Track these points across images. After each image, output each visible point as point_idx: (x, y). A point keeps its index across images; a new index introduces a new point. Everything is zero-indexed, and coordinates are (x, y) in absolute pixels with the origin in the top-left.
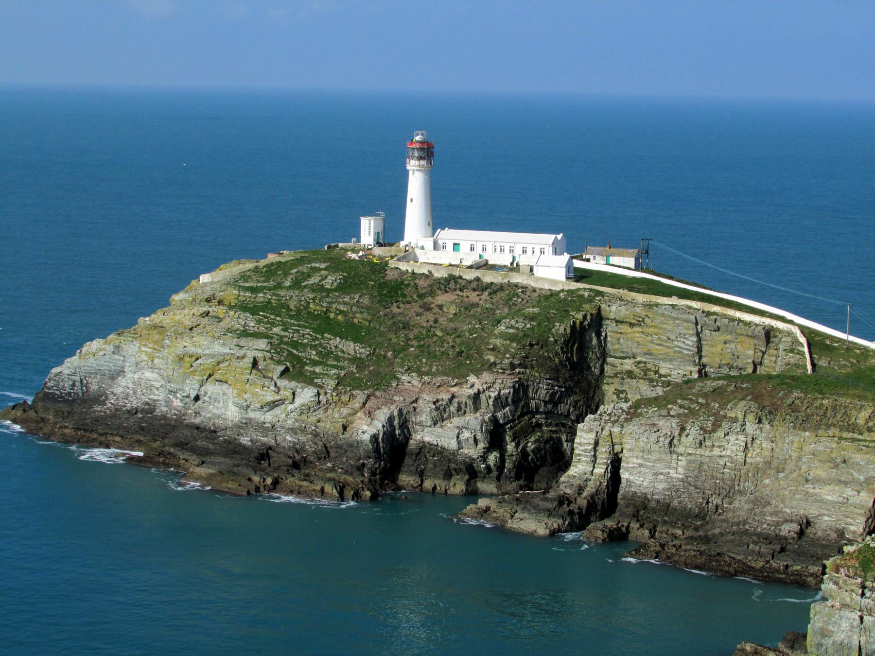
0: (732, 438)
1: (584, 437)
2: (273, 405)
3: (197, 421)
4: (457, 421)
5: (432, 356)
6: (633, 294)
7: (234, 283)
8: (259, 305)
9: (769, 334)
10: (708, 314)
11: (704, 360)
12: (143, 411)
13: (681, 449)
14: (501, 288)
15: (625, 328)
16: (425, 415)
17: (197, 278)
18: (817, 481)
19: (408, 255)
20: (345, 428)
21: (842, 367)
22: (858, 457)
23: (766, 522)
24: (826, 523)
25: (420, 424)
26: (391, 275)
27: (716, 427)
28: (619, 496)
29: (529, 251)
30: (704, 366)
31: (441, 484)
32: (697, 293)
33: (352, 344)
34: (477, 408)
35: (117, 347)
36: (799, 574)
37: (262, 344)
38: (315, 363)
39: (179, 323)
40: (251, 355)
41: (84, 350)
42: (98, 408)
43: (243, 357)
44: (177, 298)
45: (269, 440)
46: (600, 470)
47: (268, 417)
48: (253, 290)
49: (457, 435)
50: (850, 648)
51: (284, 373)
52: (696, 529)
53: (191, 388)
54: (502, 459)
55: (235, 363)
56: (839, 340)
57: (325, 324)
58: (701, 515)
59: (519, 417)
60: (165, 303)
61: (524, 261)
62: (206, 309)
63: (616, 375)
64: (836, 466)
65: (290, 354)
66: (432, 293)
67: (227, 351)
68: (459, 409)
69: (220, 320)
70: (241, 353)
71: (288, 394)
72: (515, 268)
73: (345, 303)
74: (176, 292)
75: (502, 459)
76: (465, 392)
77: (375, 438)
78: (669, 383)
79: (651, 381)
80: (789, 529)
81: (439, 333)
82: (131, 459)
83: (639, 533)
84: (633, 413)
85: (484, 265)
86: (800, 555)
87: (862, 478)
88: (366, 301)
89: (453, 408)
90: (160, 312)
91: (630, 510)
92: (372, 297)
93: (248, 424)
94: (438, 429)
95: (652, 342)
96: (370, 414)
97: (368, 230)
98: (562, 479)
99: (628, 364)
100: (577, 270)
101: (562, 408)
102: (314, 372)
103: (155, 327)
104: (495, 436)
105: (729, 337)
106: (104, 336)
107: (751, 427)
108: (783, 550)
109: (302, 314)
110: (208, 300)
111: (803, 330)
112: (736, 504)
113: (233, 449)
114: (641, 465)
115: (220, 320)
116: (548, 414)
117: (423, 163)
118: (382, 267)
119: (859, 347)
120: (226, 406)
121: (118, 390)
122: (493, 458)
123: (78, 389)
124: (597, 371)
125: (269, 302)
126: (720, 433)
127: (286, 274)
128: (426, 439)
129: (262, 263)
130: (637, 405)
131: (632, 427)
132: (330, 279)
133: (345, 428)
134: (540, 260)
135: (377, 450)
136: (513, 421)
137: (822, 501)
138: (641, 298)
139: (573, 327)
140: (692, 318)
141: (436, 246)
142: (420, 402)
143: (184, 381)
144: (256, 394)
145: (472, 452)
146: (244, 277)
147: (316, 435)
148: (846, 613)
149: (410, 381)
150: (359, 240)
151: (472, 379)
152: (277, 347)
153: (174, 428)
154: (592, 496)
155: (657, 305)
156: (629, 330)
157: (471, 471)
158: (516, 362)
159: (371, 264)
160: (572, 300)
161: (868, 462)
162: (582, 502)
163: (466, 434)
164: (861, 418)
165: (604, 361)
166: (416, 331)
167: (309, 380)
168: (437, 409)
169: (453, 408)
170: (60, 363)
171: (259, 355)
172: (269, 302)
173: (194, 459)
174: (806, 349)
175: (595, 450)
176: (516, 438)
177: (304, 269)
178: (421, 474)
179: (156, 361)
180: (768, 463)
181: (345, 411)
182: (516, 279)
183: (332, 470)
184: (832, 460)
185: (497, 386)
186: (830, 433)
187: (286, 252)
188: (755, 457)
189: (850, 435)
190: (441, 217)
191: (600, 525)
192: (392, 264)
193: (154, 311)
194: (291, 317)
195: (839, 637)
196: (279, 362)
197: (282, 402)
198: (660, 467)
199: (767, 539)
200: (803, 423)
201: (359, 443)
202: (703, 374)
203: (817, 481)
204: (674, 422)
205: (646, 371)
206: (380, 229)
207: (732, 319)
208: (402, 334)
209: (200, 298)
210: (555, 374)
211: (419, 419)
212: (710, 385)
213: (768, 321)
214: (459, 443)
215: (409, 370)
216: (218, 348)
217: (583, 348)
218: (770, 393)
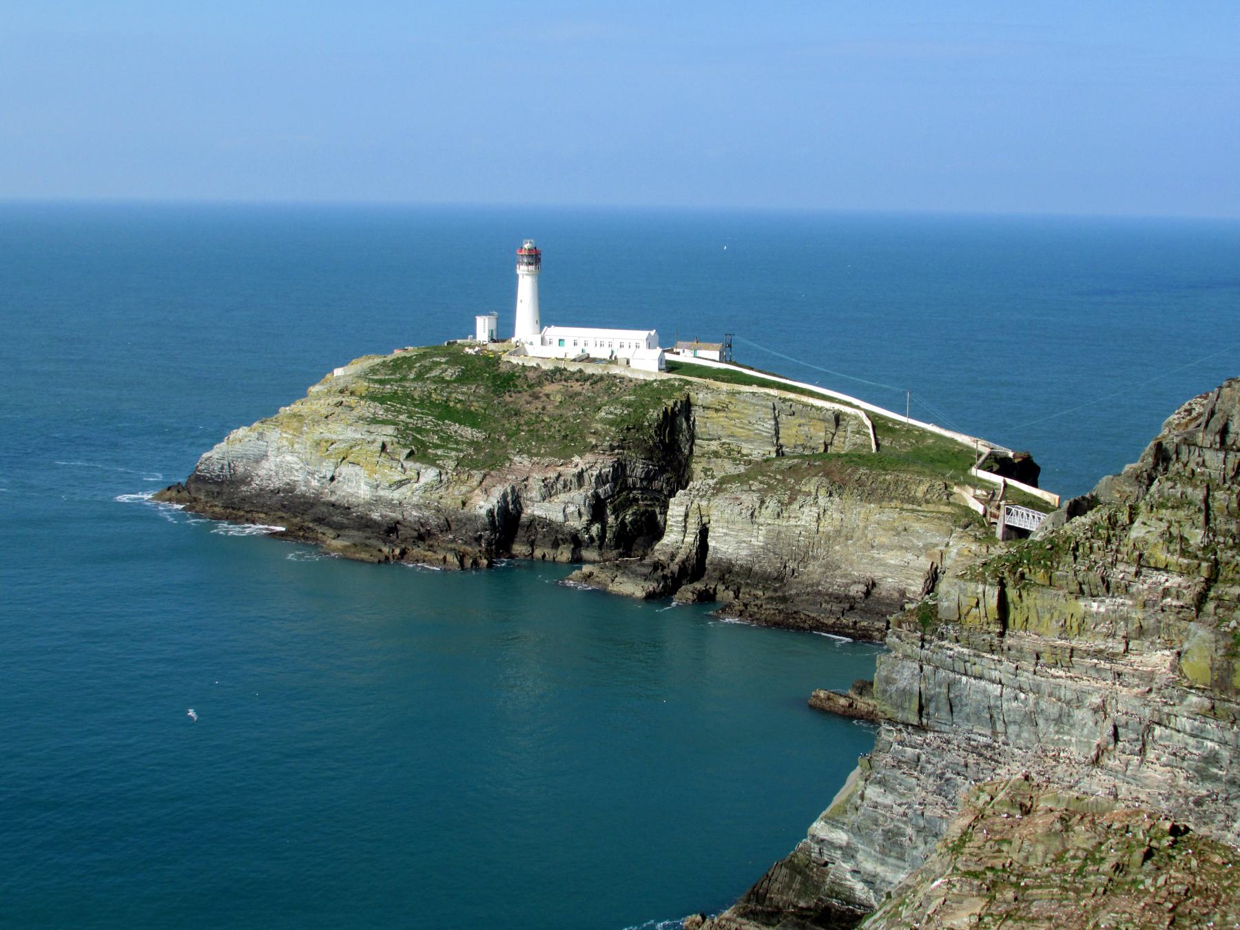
0: (806, 510)
1: (676, 509)
2: (400, 484)
3: (333, 499)
4: (563, 497)
5: (540, 439)
6: (718, 383)
7: (364, 376)
8: (387, 395)
9: (838, 418)
10: (785, 400)
11: (781, 441)
12: (284, 491)
13: (761, 520)
14: (601, 378)
15: (711, 413)
16: (535, 491)
17: (331, 371)
18: (882, 547)
19: (519, 350)
20: (464, 504)
21: (903, 446)
22: (917, 526)
23: (836, 584)
24: (889, 584)
25: (531, 499)
26: (504, 368)
27: (792, 499)
28: (707, 561)
29: (626, 346)
30: (781, 446)
31: (550, 553)
32: (774, 382)
33: (469, 430)
34: (580, 485)
35: (261, 434)
36: (866, 629)
37: (390, 430)
38: (437, 447)
39: (316, 411)
40: (380, 439)
41: (232, 437)
42: (244, 488)
43: (373, 442)
44: (314, 389)
45: (397, 515)
46: (690, 539)
47: (396, 495)
48: (381, 382)
49: (564, 509)
50: (911, 694)
51: (410, 455)
52: (775, 590)
53: (327, 470)
54: (603, 530)
55: (366, 447)
56: (900, 423)
57: (446, 412)
58: (780, 578)
59: (618, 493)
60: (303, 394)
61: (621, 354)
62: (340, 399)
63: (703, 455)
64: (898, 534)
65: (415, 438)
66: (540, 384)
67: (358, 436)
69: (352, 408)
70: (372, 438)
71: (414, 474)
72: (613, 361)
73: (463, 393)
74: (314, 384)
75: (603, 530)
76: (570, 471)
77: (491, 512)
78: (750, 462)
79: (735, 460)
80: (857, 590)
81: (546, 419)
82: (274, 534)
83: (725, 595)
84: (718, 489)
85: (588, 359)
86: (866, 612)
87: (921, 544)
88: (482, 391)
89: (559, 486)
90: (298, 403)
91: (717, 574)
92: (487, 387)
93: (378, 501)
94: (546, 504)
95: (735, 425)
96: (486, 491)
97: (483, 327)
98: (657, 547)
99: (714, 446)
100: (668, 362)
101: (656, 485)
102: (436, 455)
103: (295, 415)
104: (597, 510)
105: (803, 421)
106: (249, 424)
107: (822, 501)
108: (852, 608)
109: (425, 403)
110: (342, 392)
111: (869, 414)
112: (810, 568)
113: (365, 524)
114: (726, 534)
115: (352, 408)
116: (644, 490)
117: (532, 268)
118: (494, 361)
119: (918, 429)
120: (358, 486)
121: (262, 472)
122: (595, 529)
123: (226, 472)
124: (686, 452)
125: (396, 393)
126: (796, 506)
127: (410, 368)
128: (536, 513)
129: (389, 358)
130: (723, 481)
131: (716, 501)
132: (450, 372)
133: (464, 504)
134: (635, 354)
135: (492, 523)
136: (612, 496)
137: (885, 565)
138: (725, 387)
139: (665, 413)
140: (770, 404)
141: (543, 342)
142: (531, 480)
143: (320, 464)
144: (384, 475)
145: (576, 524)
146: (373, 370)
147: (438, 510)
148: (908, 663)
149: (521, 462)
150: (475, 337)
151: (576, 459)
152: (403, 432)
153: (312, 505)
154: (683, 562)
155: (739, 393)
156: (715, 415)
157: (576, 541)
158: (615, 444)
159: (487, 358)
160: (664, 389)
161: (927, 531)
162: (674, 567)
163: (571, 509)
164: (920, 491)
165: (693, 443)
166: (526, 418)
167: (432, 462)
168: (546, 486)
169: (559, 486)
170: (210, 447)
171: (387, 439)
172: (396, 393)
173: (330, 533)
174: (871, 431)
175: (685, 521)
176: (616, 511)
177: (427, 362)
178: (532, 544)
179: (296, 446)
180: (838, 532)
181: (464, 489)
182: (615, 370)
183: (453, 541)
184: (894, 529)
185: (599, 466)
186: (893, 505)
187: (410, 348)
188: (827, 526)
189: (910, 506)
190: (548, 316)
191: (690, 587)
192: (505, 358)
193: (294, 402)
194: (415, 406)
195: (902, 684)
196: (405, 446)
197: (408, 481)
198: (743, 536)
199: (838, 598)
200: (869, 496)
201: (477, 517)
202: (780, 454)
203: (882, 547)
204: (755, 496)
205: (730, 451)
206: (494, 327)
207: (805, 405)
208: (514, 420)
209: (334, 389)
210: (649, 454)
211: (529, 495)
212: (787, 462)
213: (837, 407)
214: (565, 516)
215: (520, 452)
216: (351, 434)
218: (839, 470)
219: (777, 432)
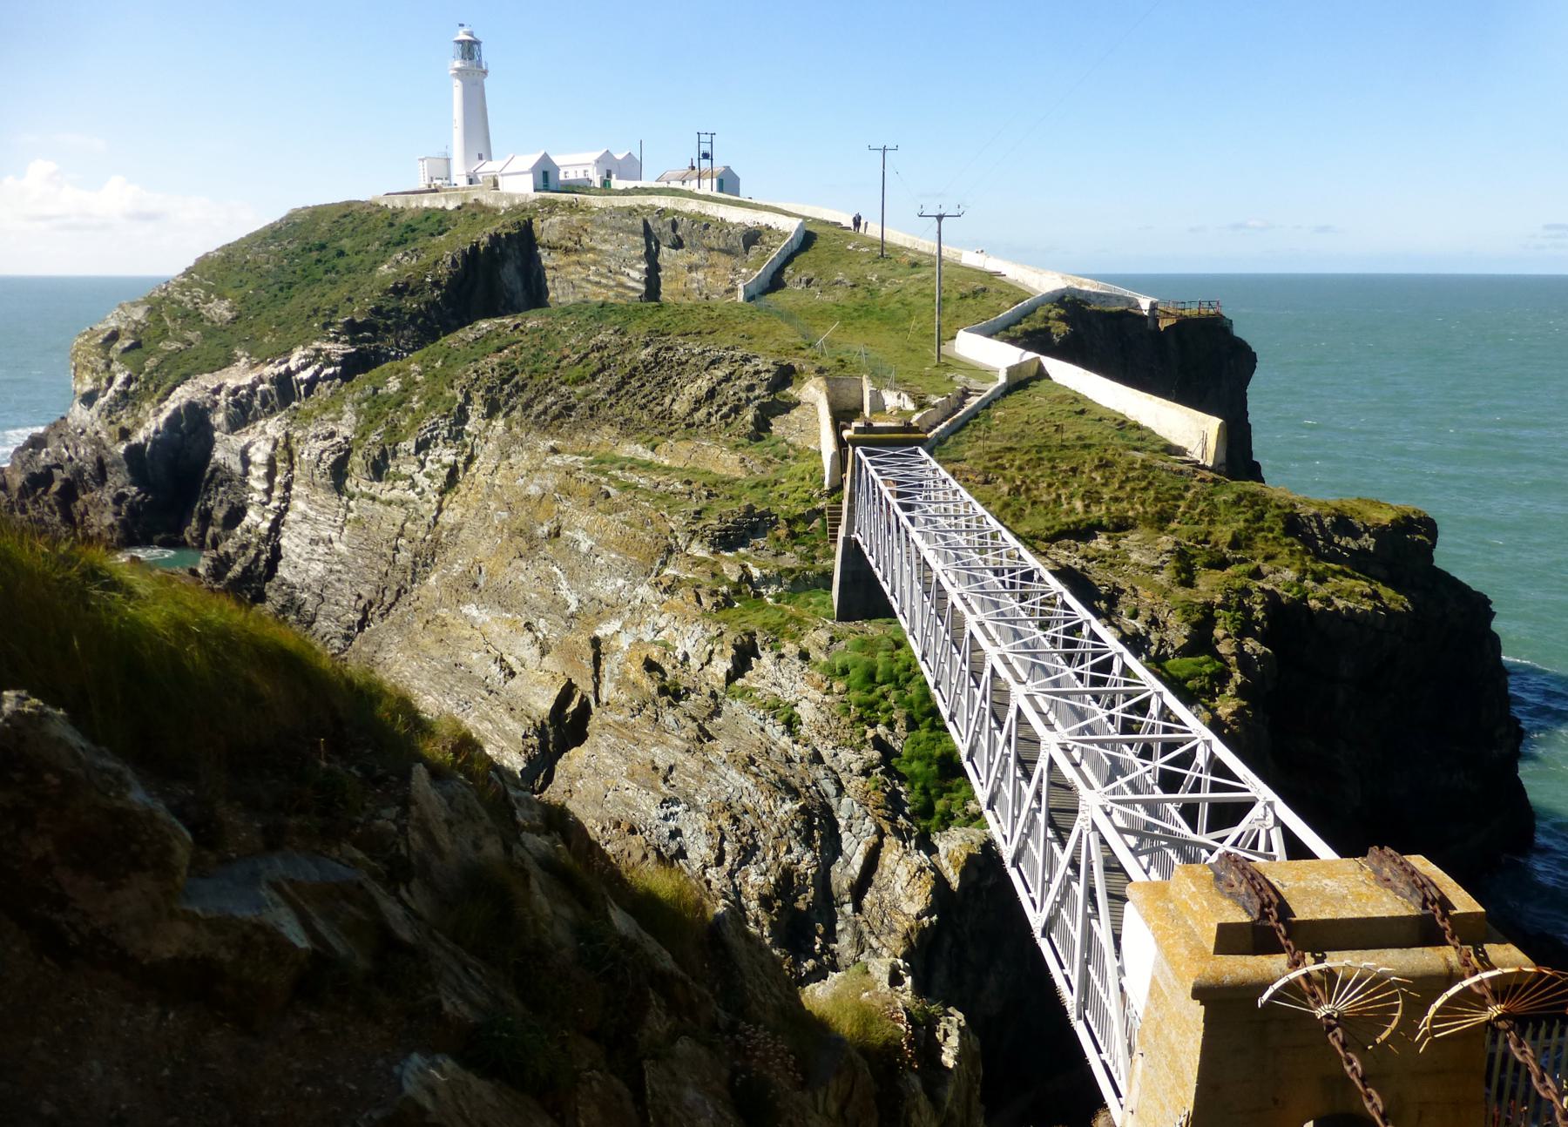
46: (266, 525)
68: (264, 403)
105: (695, 258)
168: (237, 403)
169: (257, 403)
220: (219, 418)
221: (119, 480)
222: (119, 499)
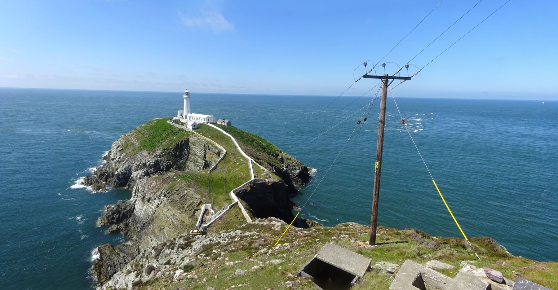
76: (143, 162)
77: (118, 174)
139: (178, 145)
217: (182, 151)
219: (205, 155)
220: (133, 169)
221: (115, 179)
222: (115, 182)
